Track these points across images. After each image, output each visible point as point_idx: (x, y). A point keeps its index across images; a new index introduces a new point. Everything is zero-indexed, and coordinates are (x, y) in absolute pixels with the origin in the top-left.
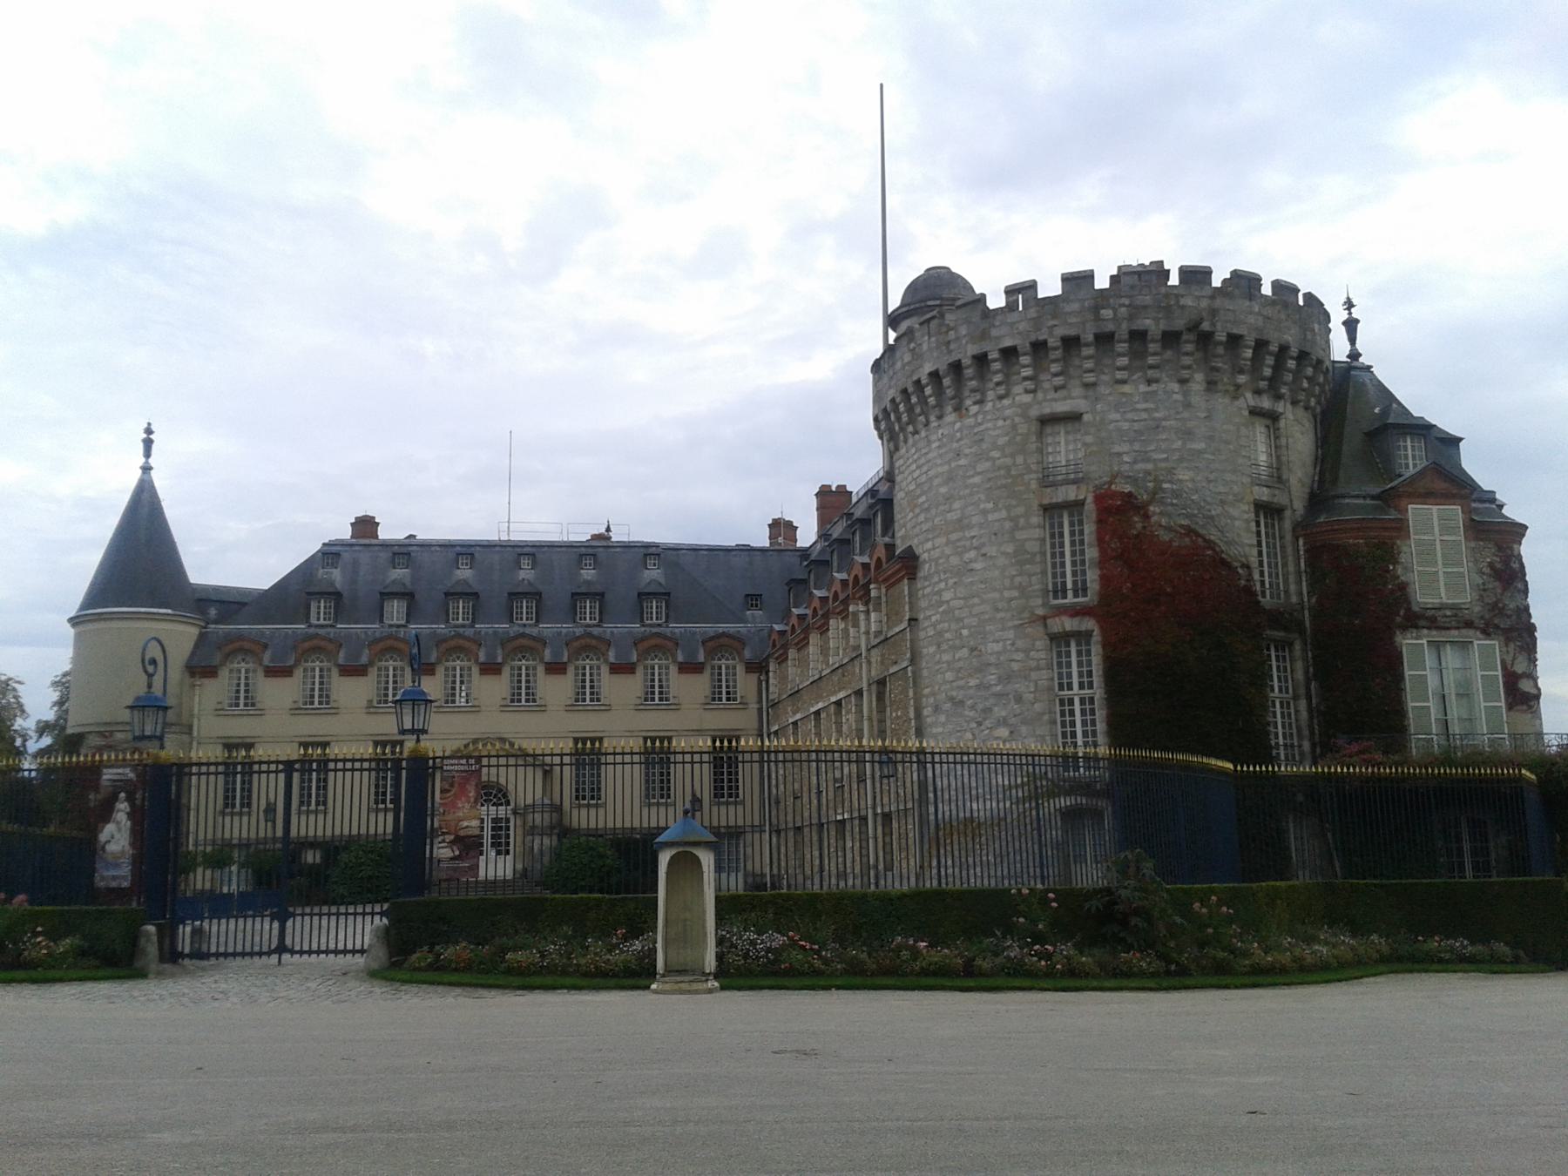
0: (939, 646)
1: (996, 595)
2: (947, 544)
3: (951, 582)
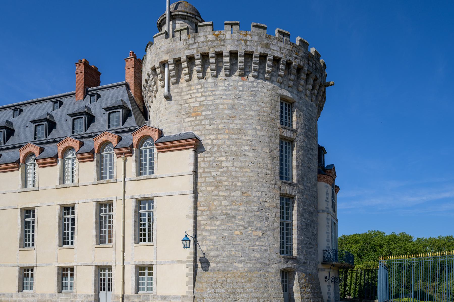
0: (217, 188)
1: (260, 170)
2: (228, 139)
3: (229, 158)
